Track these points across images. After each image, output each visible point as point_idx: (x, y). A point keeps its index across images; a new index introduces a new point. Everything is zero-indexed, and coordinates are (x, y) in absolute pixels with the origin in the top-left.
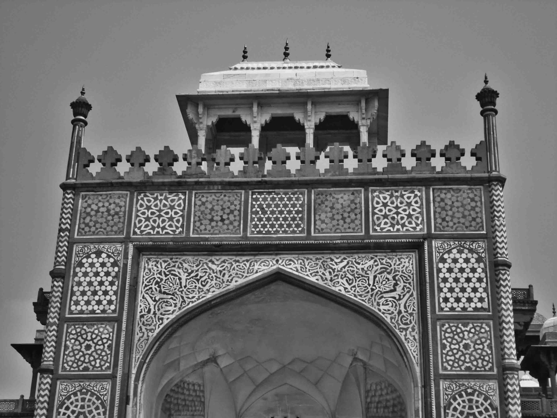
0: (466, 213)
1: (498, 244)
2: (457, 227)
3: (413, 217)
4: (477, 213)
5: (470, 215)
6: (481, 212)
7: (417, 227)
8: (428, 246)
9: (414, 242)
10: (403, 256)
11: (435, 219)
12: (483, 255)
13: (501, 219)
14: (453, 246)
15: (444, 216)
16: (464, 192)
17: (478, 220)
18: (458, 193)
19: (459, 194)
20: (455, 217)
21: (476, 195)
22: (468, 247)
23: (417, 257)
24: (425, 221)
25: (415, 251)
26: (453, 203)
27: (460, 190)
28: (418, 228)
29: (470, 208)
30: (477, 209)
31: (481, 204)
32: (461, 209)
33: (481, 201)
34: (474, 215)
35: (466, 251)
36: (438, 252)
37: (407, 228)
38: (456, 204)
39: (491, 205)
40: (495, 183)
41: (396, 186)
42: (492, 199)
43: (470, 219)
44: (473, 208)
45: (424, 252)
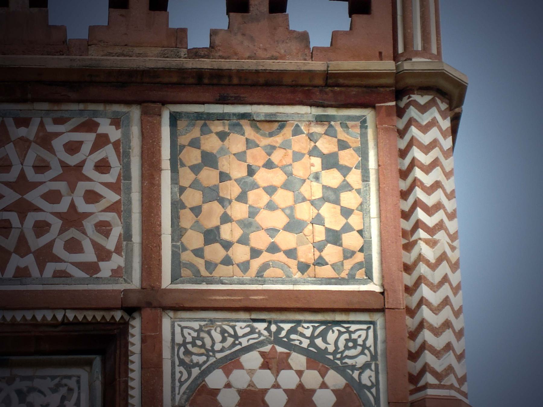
0: (305, 212)
1: (427, 335)
2: (265, 267)
3: (89, 225)
4: (346, 212)
5: (318, 220)
6: (363, 208)
7: (102, 264)
8: (143, 340)
9: (85, 323)
10: (37, 383)
11: (178, 232)
12: (367, 378)
13: (441, 236)
14: (244, 342)
15: (215, 222)
16: (297, 131)
17: (351, 240)
18: (271, 135)
19: (278, 140)
20: (259, 228)
21: (343, 145)
22: (305, 343)
23: (98, 385)
24: (136, 238)
25: (89, 363)
26: (251, 171)
27: (282, 124)
28: (106, 269)
29: (317, 193)
30: (349, 199)
31: (365, 178)
32: (283, 198)
33: (364, 167)
34: (332, 218)
35: (298, 360)
36: (182, 363)
37: (60, 266)
38: (263, 177)
39: (404, 185)
40: (422, 100)
41: (24, 101)
42: (407, 161)
43: (320, 234)
44: (332, 195)
45: (127, 362)
